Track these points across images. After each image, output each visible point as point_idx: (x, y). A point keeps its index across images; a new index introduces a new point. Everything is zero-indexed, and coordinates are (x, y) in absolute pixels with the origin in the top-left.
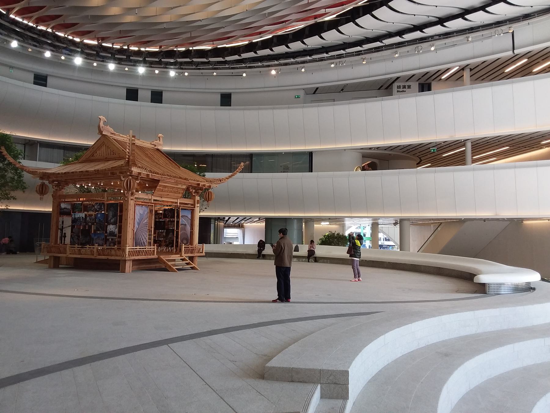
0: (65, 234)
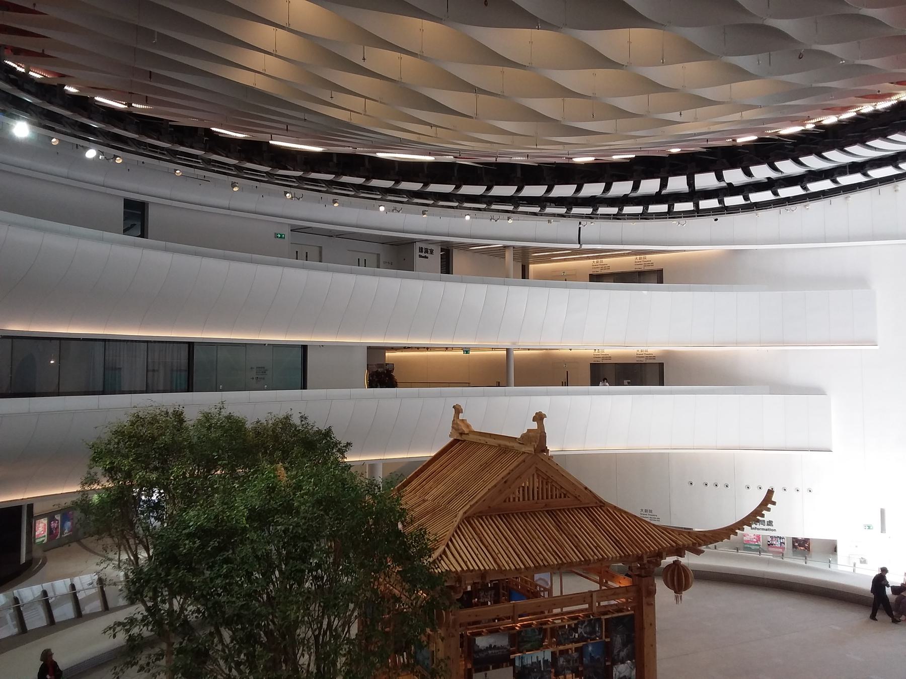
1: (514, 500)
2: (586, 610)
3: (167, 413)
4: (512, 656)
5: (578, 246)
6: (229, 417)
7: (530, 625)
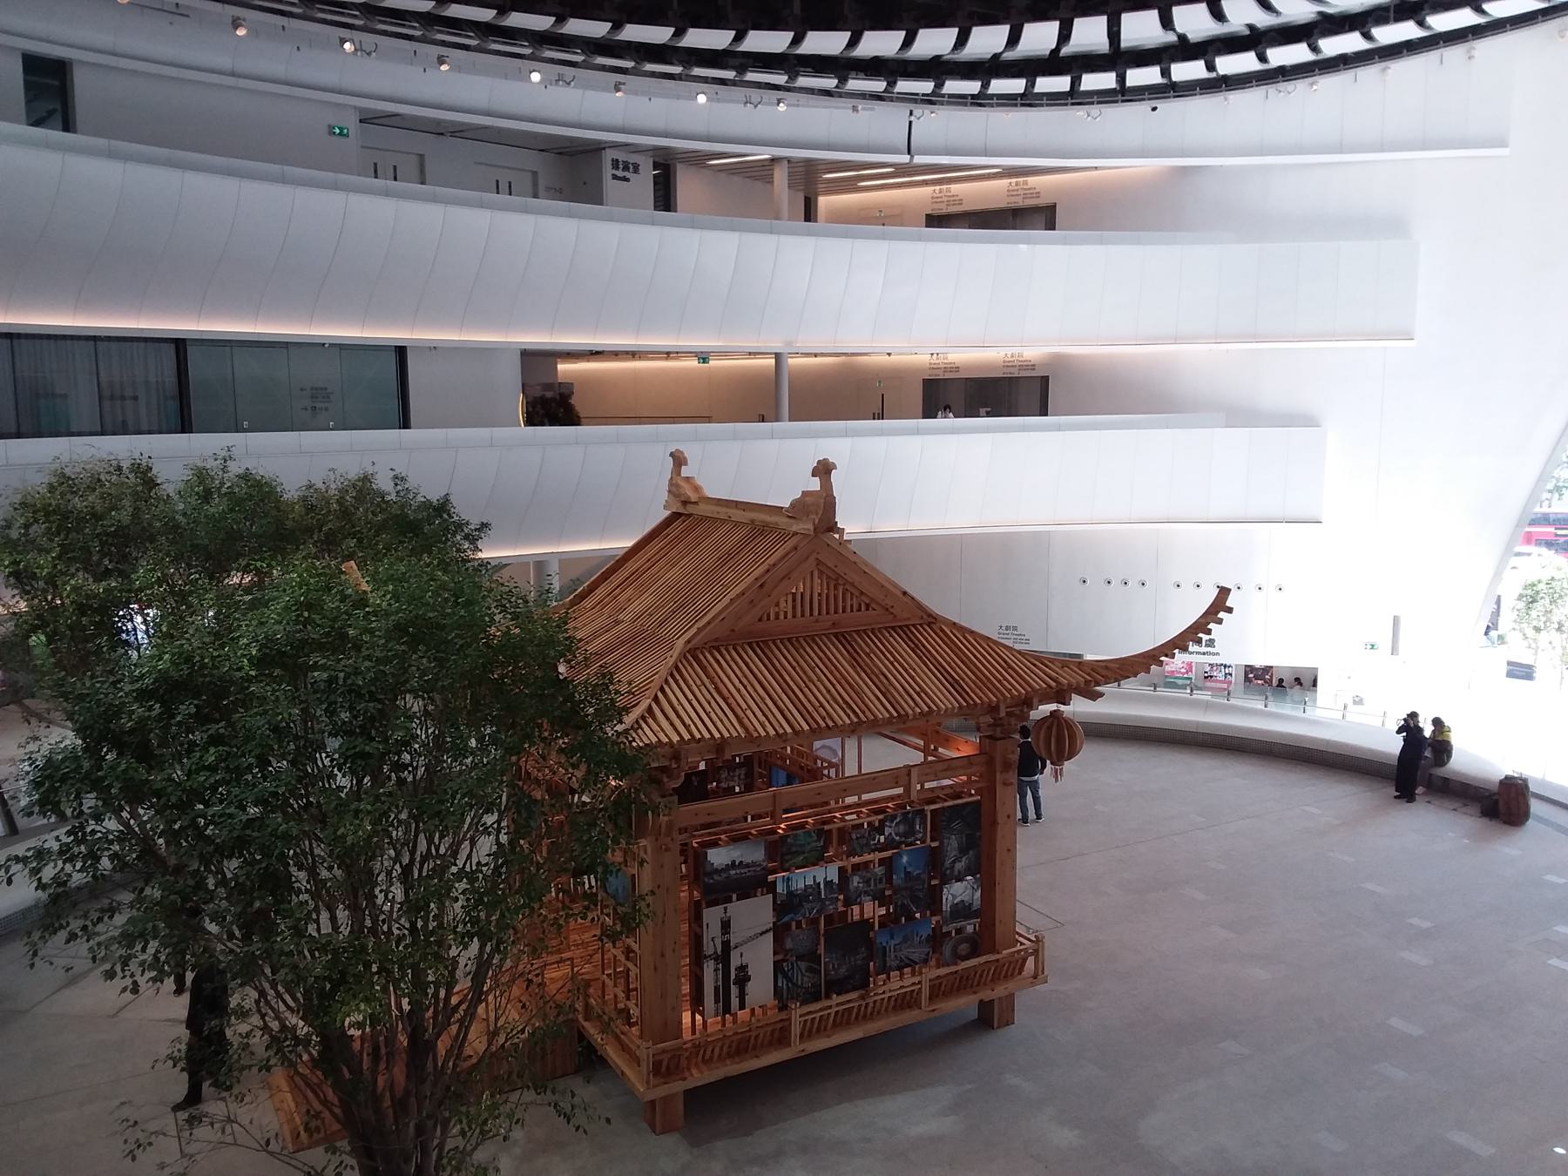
0: (742, 968)
1: (777, 618)
2: (899, 796)
3: (119, 468)
4: (771, 878)
5: (905, 159)
6: (246, 476)
7: (802, 826)
